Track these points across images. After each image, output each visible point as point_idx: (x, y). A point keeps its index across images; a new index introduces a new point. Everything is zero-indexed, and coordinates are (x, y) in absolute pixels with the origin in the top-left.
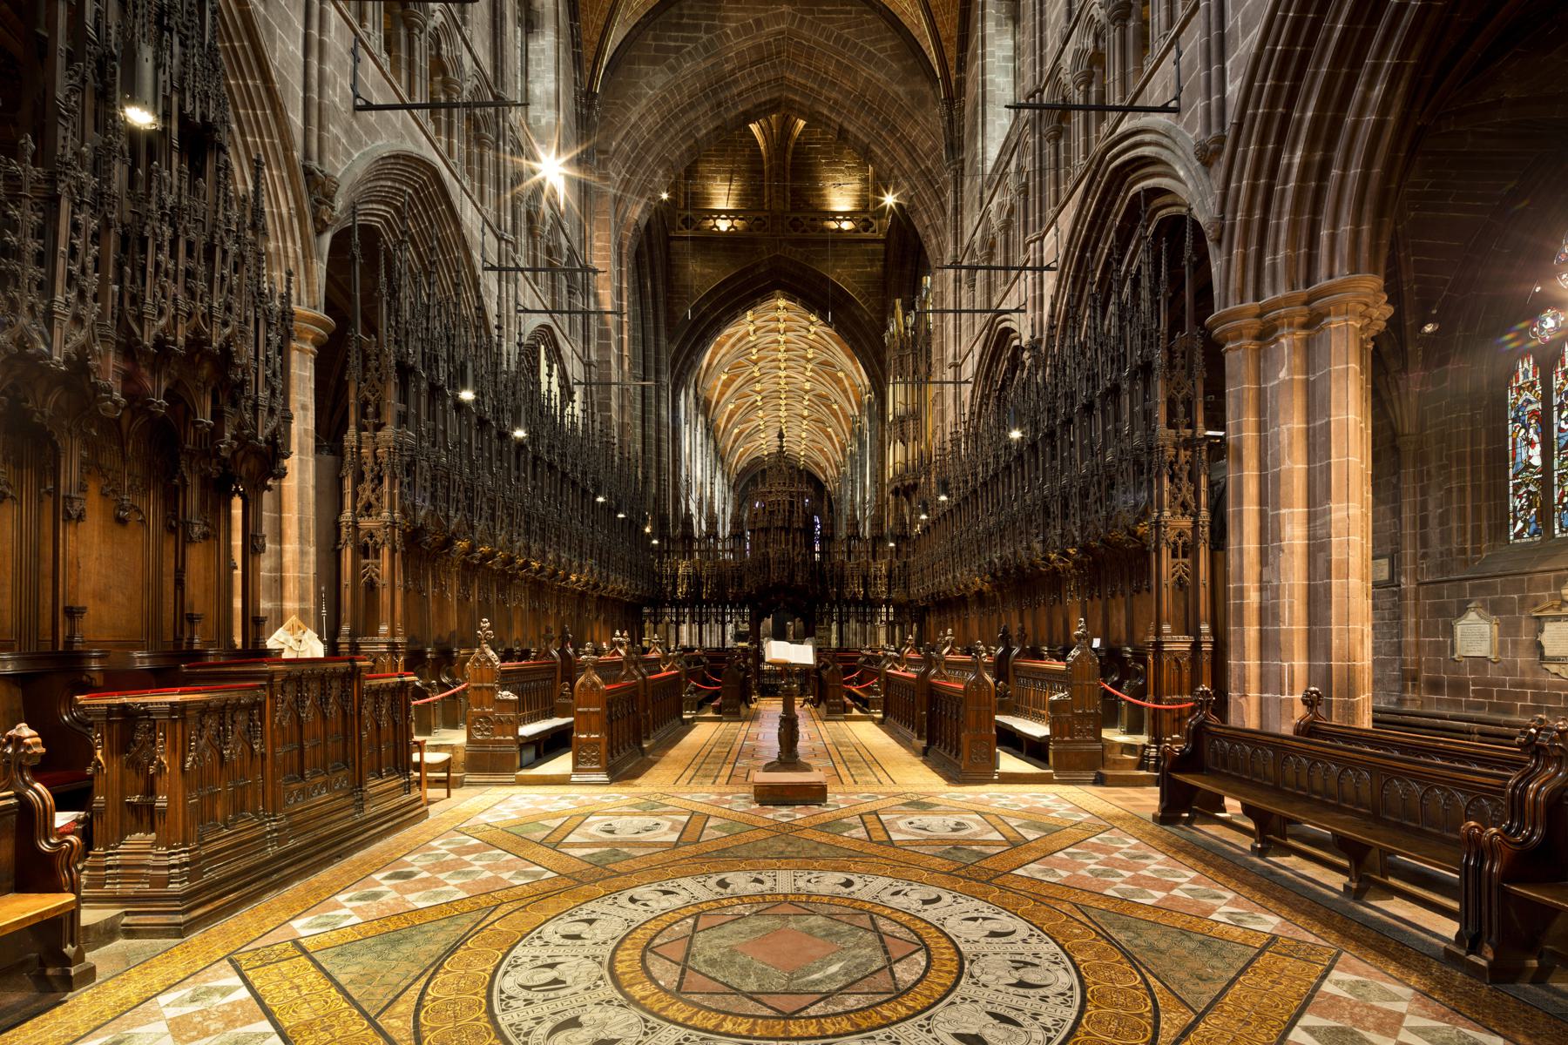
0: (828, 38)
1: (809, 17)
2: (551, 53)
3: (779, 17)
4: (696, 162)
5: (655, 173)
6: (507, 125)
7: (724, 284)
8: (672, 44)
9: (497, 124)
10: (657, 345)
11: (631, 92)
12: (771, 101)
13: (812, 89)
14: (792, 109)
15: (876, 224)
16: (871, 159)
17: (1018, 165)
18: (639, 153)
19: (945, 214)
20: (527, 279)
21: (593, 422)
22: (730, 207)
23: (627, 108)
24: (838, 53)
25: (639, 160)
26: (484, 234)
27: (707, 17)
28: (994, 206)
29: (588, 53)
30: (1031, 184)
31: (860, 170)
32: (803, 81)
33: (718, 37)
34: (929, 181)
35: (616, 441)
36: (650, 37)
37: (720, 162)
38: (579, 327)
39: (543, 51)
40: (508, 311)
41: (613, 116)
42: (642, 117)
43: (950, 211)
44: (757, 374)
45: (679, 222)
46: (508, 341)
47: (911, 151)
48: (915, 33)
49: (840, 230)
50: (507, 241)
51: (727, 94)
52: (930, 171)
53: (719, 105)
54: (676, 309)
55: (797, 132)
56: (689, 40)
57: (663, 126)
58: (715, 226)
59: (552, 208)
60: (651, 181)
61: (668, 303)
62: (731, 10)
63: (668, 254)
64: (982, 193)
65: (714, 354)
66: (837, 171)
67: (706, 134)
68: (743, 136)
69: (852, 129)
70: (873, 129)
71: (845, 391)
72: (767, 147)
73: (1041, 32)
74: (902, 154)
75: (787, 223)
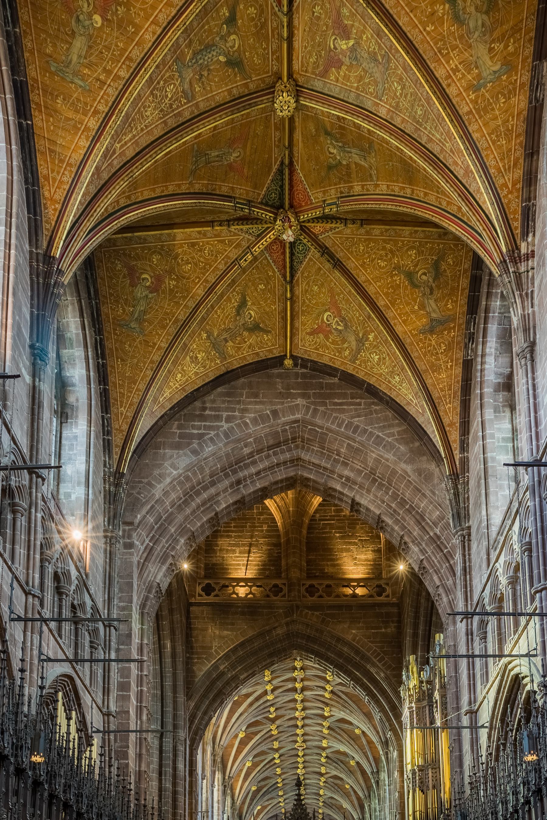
0: (340, 426)
1: (322, 408)
2: (83, 439)
3: (294, 409)
4: (216, 535)
5: (176, 541)
6: (40, 495)
7: (242, 644)
8: (196, 432)
9: (31, 494)
10: (175, 702)
11: (156, 472)
12: (287, 479)
13: (325, 469)
14: (307, 486)
15: (389, 590)
16: (382, 528)
17: (520, 528)
18: (162, 524)
19: (455, 575)
20: (50, 631)
21: (110, 766)
22: (249, 575)
23: (150, 484)
24: (348, 438)
25: (162, 531)
26: (12, 589)
28: (500, 566)
29: (117, 440)
30: (534, 541)
31: (373, 543)
32: (317, 462)
33: (238, 425)
34: (438, 546)
35: (132, 787)
36: (175, 426)
37: (239, 537)
38: (100, 680)
39: (76, 437)
40: (31, 659)
41: (139, 493)
42: (166, 494)
43: (459, 569)
44: (275, 732)
45: (199, 589)
46: (30, 686)
47: (420, 520)
48: (420, 420)
49: (354, 595)
50: (34, 596)
51: (246, 473)
52: (439, 538)
53: (239, 482)
54: (195, 668)
55: (312, 510)
56: (210, 428)
57: (186, 500)
58: (234, 593)
59: (79, 571)
60: (174, 548)
61: (187, 663)
62: (250, 403)
63: (188, 618)
64: (488, 554)
65: (232, 712)
66: (350, 543)
67: (226, 508)
68: (261, 514)
69: (363, 502)
70: (383, 502)
71: (362, 748)
72: (284, 524)
73: (536, 412)
74: (412, 523)
75: (303, 589)
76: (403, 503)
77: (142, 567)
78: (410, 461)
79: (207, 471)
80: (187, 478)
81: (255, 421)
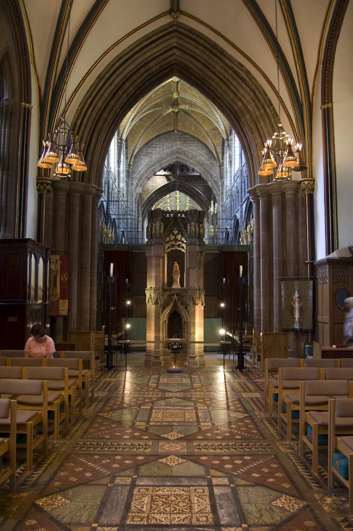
27: (159, 145)
42: (142, 169)
47: (211, 175)
56: (154, 150)
76: (207, 170)
77: (136, 189)
78: (208, 160)
79: (153, 162)
80: (148, 164)
81: (166, 149)
